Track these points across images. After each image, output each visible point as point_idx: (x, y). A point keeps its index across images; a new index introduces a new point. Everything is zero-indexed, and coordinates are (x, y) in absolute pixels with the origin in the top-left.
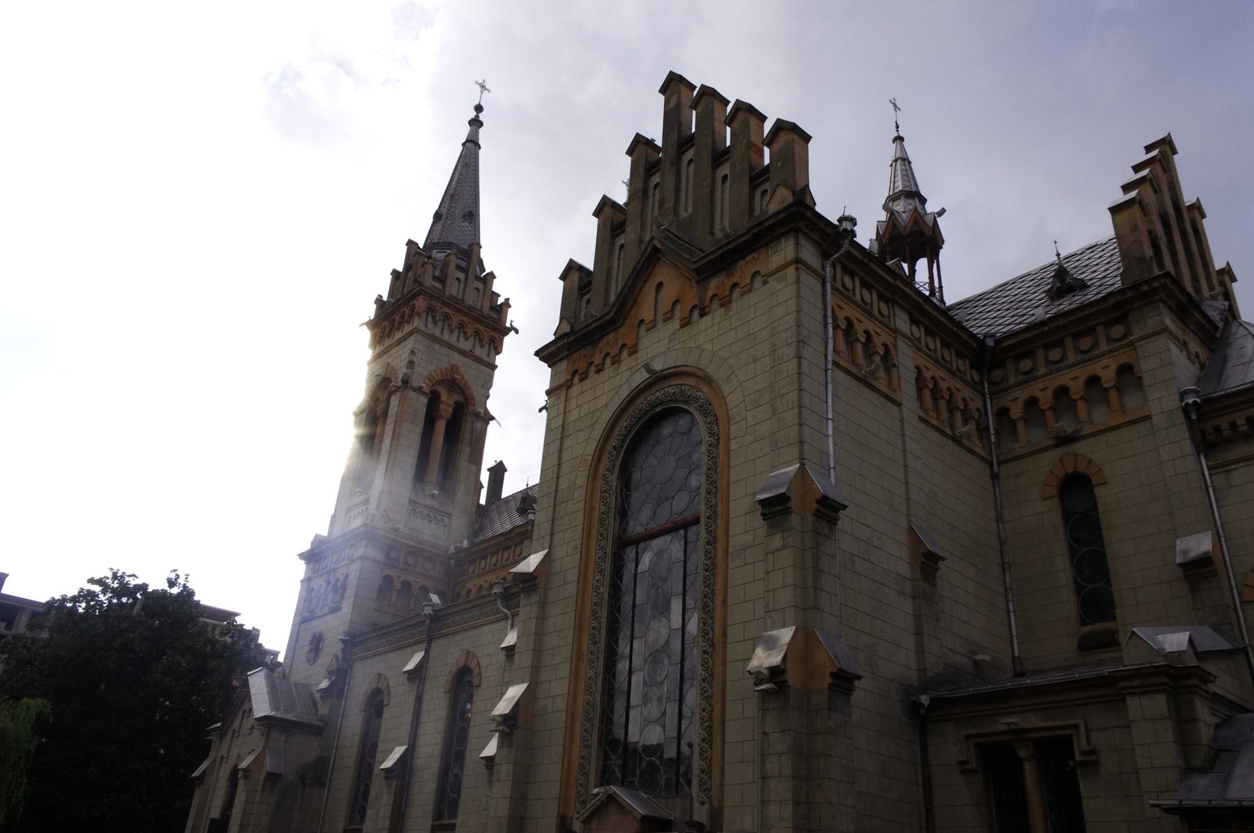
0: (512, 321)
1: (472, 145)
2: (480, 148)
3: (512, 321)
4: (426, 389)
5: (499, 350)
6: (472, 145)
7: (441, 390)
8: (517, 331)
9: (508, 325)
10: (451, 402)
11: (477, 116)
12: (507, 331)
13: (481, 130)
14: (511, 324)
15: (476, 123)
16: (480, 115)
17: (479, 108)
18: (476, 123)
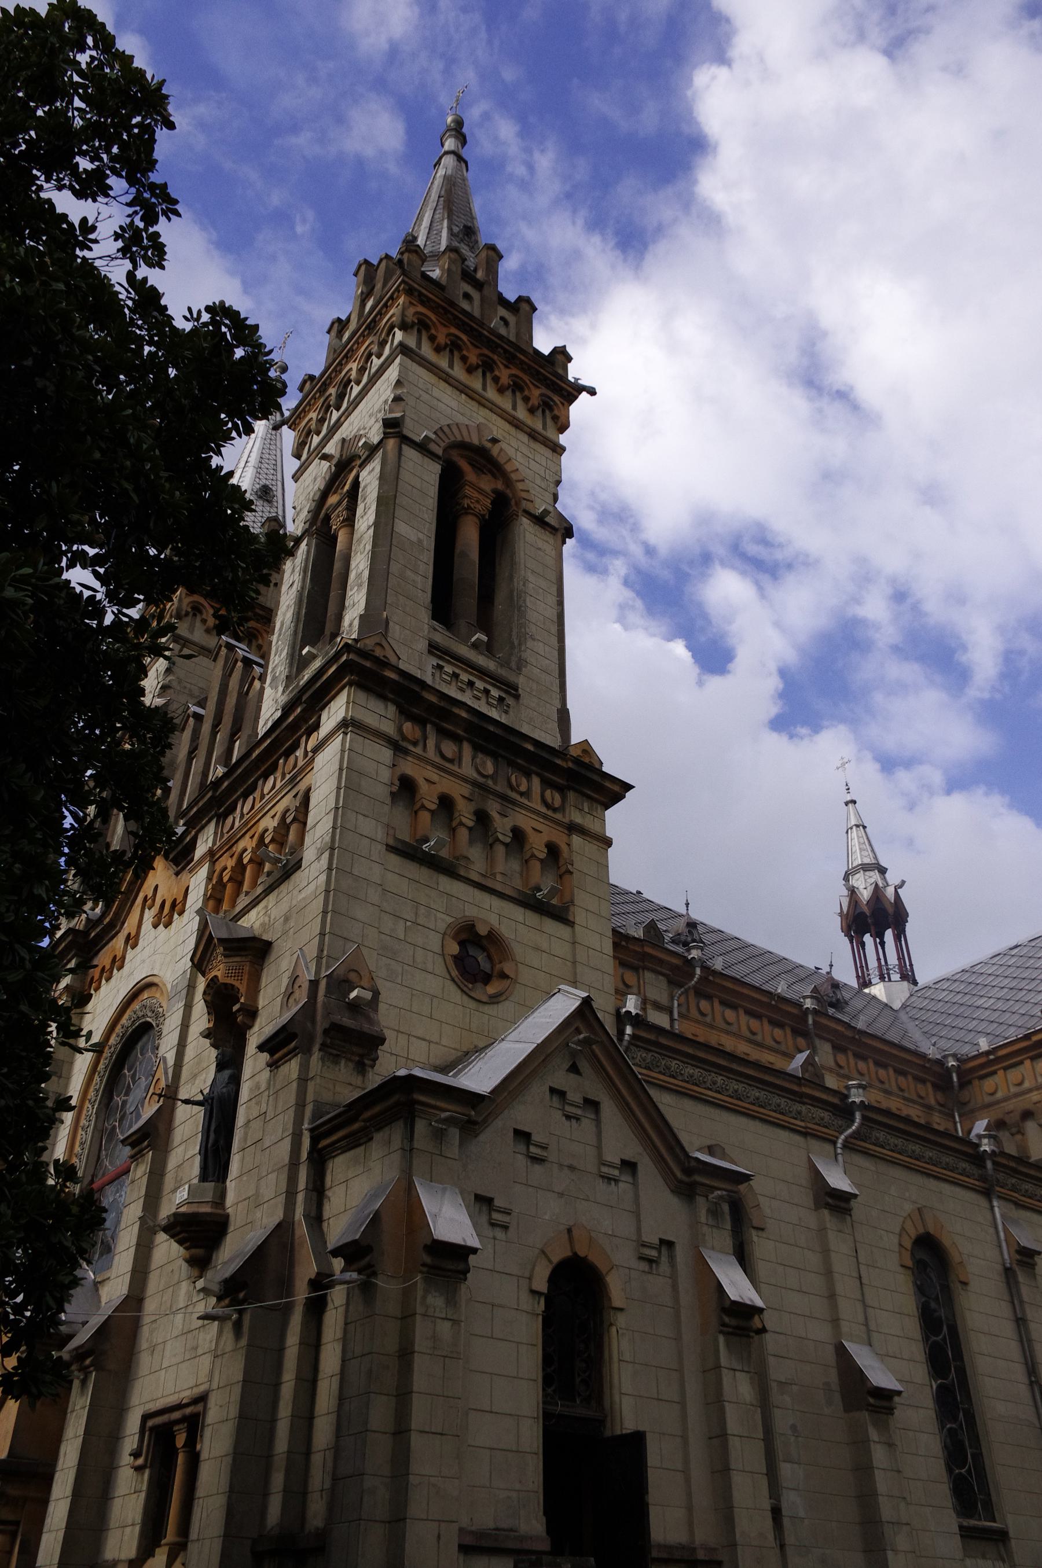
5: (562, 419)
8: (592, 392)
12: (576, 390)
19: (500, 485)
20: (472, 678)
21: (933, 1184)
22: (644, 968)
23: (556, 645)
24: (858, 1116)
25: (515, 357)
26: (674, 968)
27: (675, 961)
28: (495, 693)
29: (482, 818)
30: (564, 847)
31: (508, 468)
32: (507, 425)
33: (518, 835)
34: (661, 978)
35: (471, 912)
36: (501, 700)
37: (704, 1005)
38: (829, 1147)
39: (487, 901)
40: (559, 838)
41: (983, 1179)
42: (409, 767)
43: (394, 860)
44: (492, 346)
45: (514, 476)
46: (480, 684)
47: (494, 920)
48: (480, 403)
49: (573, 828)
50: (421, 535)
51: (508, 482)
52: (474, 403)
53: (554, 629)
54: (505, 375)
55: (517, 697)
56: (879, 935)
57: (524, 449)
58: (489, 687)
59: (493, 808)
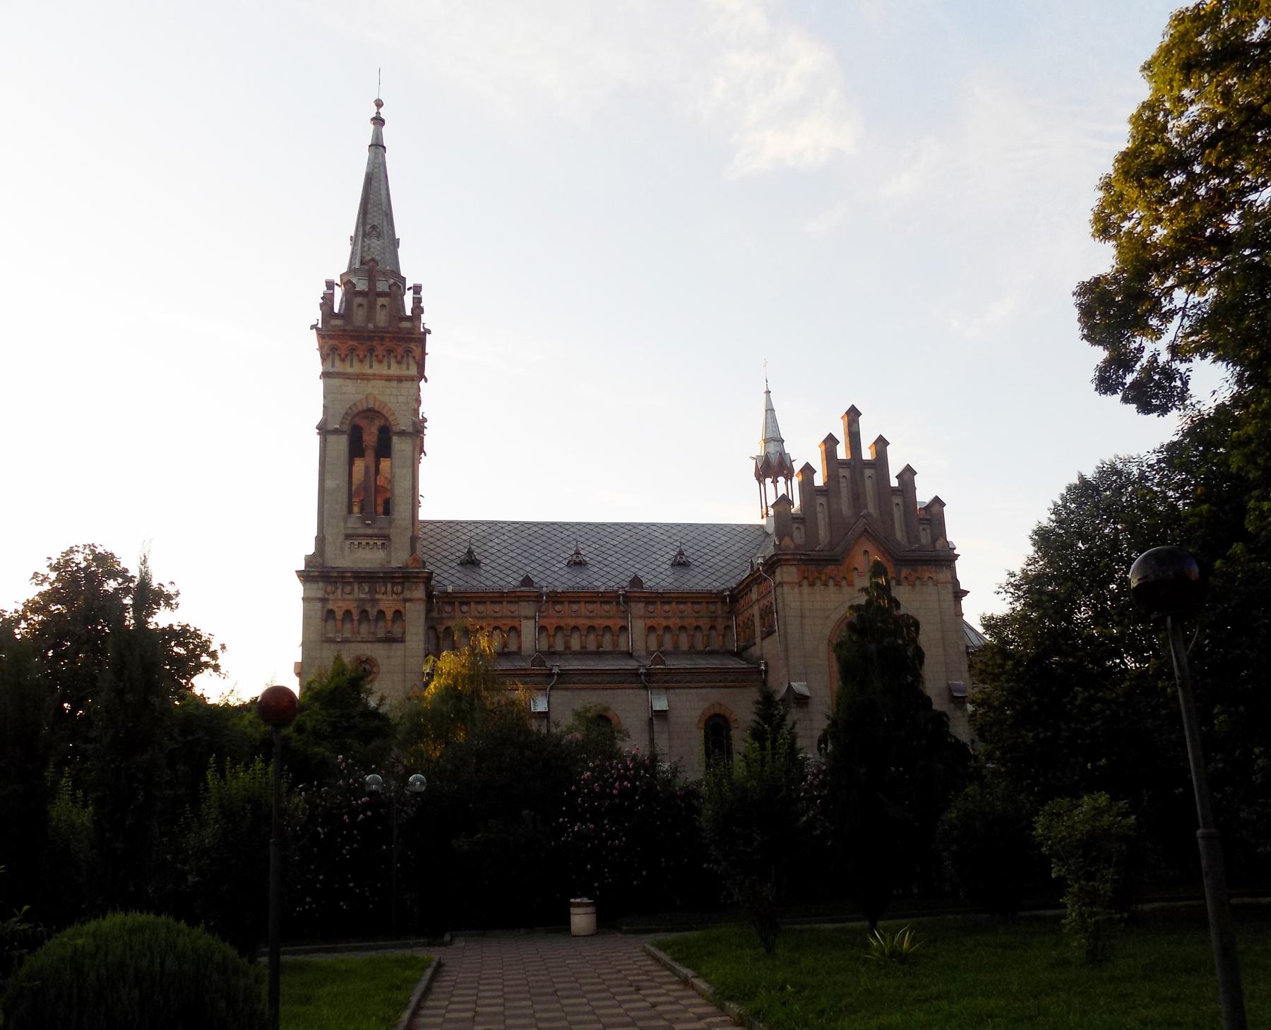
0: (424, 324)
1: (377, 146)
2: (384, 148)
3: (424, 324)
4: (346, 428)
6: (377, 146)
7: (363, 423)
8: (430, 333)
9: (422, 330)
10: (375, 430)
11: (378, 113)
13: (385, 129)
14: (424, 327)
15: (378, 121)
16: (381, 110)
17: (379, 104)
18: (378, 121)
19: (382, 422)
20: (367, 541)
21: (609, 692)
22: (521, 601)
23: (410, 501)
24: (555, 677)
25: (383, 337)
26: (536, 597)
27: (536, 594)
28: (379, 543)
29: (364, 613)
30: (402, 609)
31: (384, 412)
32: (384, 382)
33: (381, 613)
34: (531, 603)
35: (359, 653)
36: (383, 544)
37: (558, 607)
38: (544, 692)
39: (364, 646)
40: (399, 606)
41: (642, 683)
42: (330, 606)
43: (326, 645)
44: (371, 338)
45: (387, 415)
46: (371, 542)
47: (369, 653)
48: (368, 380)
49: (406, 600)
50: (338, 482)
51: (387, 419)
52: (365, 381)
53: (410, 493)
54: (380, 350)
55: (390, 540)
56: (775, 482)
57: (395, 392)
58: (376, 542)
59: (368, 608)
